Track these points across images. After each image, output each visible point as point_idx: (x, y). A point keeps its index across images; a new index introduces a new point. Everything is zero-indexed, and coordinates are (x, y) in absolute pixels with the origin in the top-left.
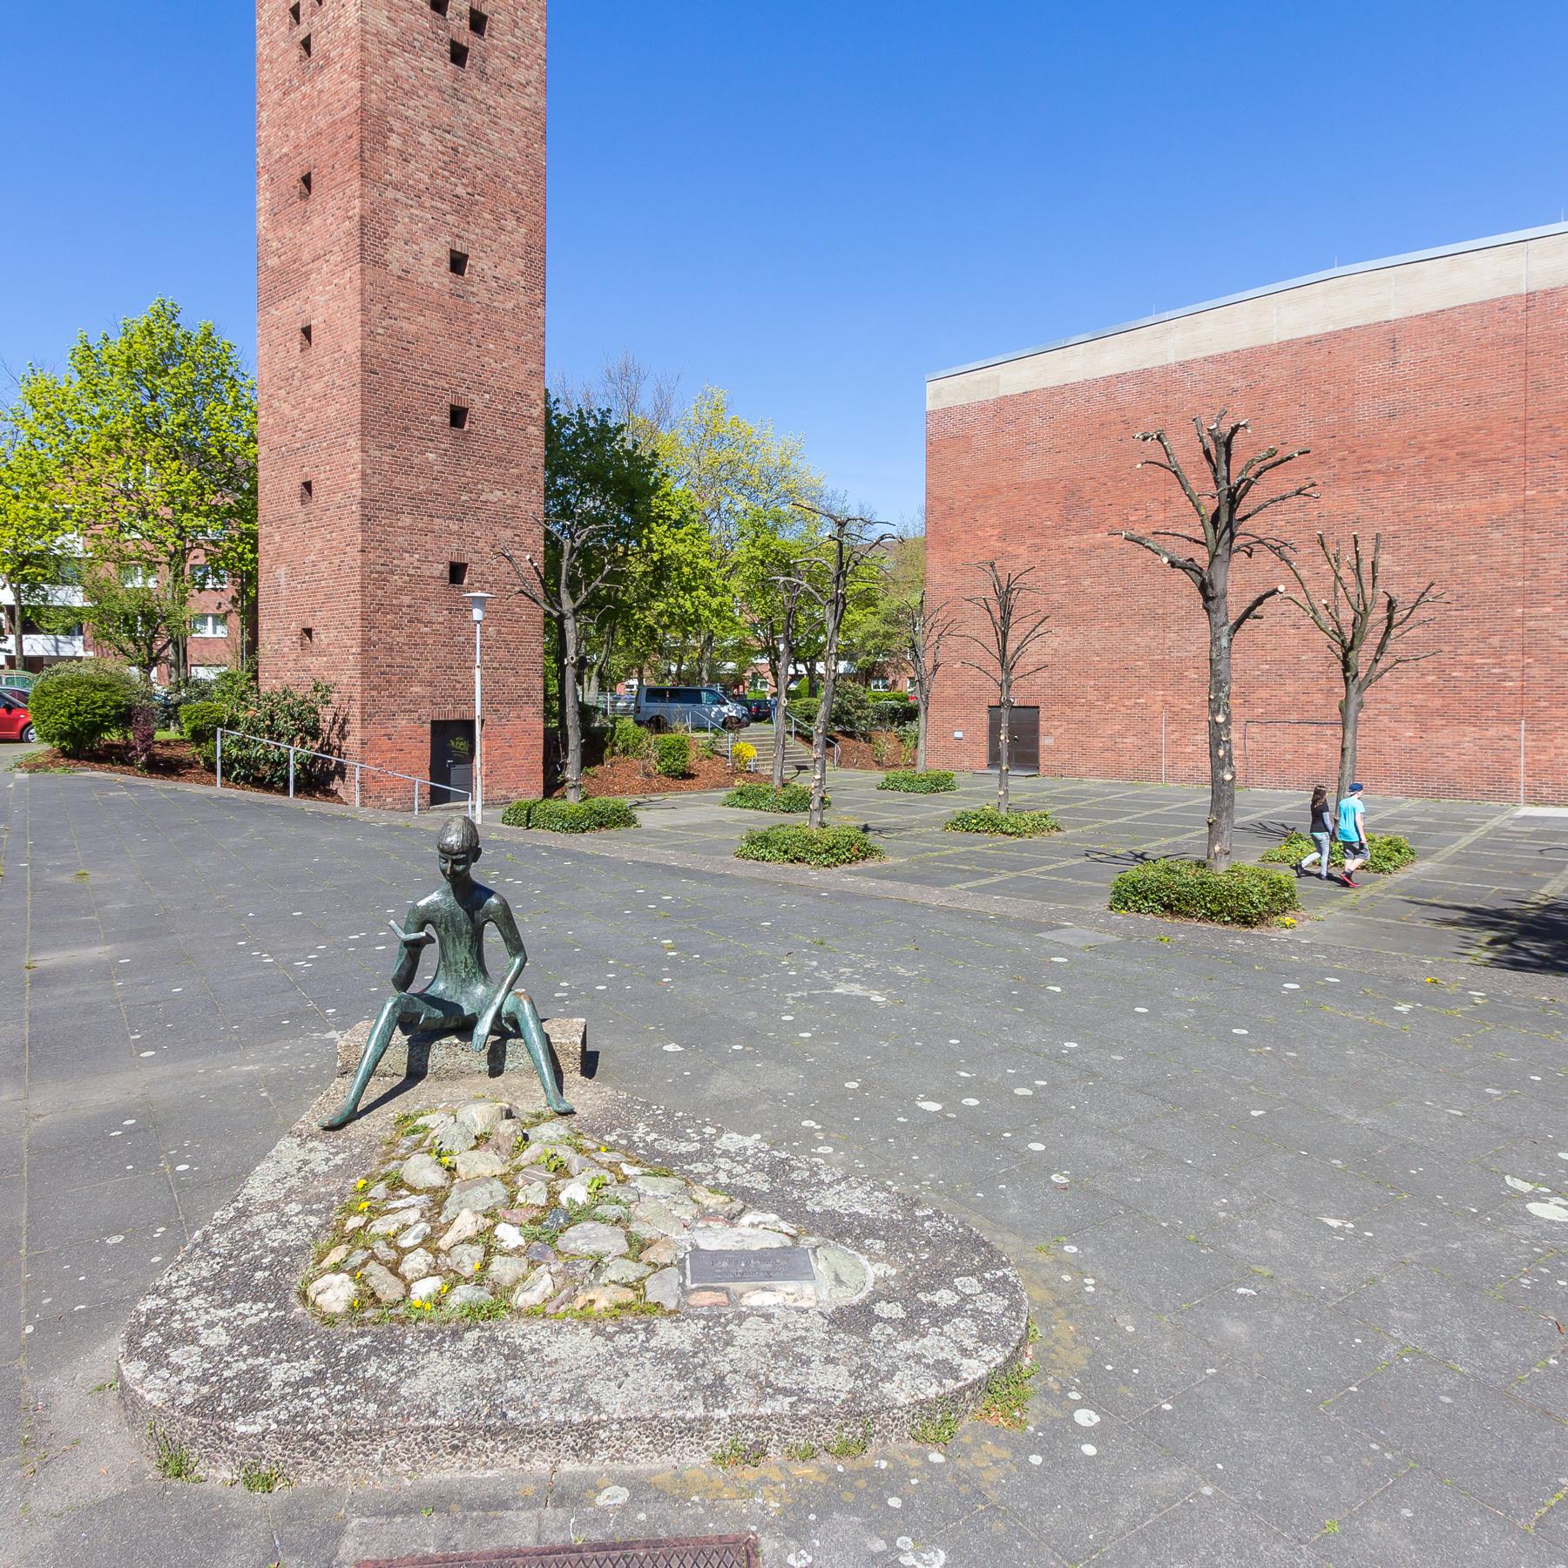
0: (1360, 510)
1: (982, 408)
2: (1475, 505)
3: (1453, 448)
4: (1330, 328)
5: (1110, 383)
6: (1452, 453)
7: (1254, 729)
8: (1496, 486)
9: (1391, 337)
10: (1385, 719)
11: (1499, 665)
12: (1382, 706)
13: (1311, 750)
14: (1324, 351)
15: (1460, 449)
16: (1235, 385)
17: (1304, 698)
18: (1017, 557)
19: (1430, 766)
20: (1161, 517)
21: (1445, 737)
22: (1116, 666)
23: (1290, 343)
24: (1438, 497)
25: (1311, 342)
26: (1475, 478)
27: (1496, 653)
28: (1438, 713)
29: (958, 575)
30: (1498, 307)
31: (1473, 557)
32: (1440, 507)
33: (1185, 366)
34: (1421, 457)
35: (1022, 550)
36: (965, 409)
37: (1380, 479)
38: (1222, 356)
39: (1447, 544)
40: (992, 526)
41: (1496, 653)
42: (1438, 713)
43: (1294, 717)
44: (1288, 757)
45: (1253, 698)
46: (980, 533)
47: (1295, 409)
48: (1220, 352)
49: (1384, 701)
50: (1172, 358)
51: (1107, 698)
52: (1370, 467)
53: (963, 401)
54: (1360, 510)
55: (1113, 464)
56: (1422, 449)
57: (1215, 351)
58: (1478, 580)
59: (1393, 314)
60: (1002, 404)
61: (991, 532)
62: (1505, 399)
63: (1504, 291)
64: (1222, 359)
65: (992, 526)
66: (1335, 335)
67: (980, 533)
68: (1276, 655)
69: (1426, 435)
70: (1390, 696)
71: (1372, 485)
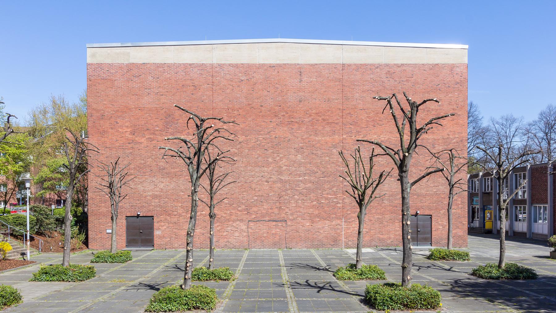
0: (290, 137)
1: (121, 67)
2: (328, 138)
3: (321, 117)
4: (278, 62)
5: (187, 67)
6: (320, 119)
7: (251, 224)
8: (334, 133)
9: (300, 70)
10: (300, 219)
11: (336, 198)
12: (298, 214)
13: (273, 232)
14: (276, 71)
15: (323, 117)
16: (242, 78)
17: (270, 211)
18: (141, 143)
19: (315, 236)
21: (319, 225)
23: (264, 65)
24: (316, 135)
25: (271, 66)
26: (328, 129)
27: (335, 194)
28: (318, 216)
29: (107, 149)
31: (327, 158)
32: (317, 139)
33: (221, 66)
34: (310, 119)
35: (143, 140)
36: (110, 65)
37: (297, 125)
38: (237, 65)
39: (319, 153)
40: (127, 127)
41: (335, 194)
42: (318, 216)
43: (267, 219)
44: (265, 235)
45: (251, 211)
46: (120, 130)
47: (265, 93)
48: (235, 63)
50: (215, 62)
52: (293, 120)
53: (109, 61)
54: (290, 137)
55: (189, 105)
56: (311, 116)
57: (234, 62)
58: (329, 166)
59: (301, 61)
60: (130, 67)
61: (126, 129)
62: (336, 101)
63: (335, 62)
64: (236, 66)
66: (279, 65)
67: (120, 130)
68: (260, 193)
69: (312, 110)
70: (301, 210)
71: (294, 127)
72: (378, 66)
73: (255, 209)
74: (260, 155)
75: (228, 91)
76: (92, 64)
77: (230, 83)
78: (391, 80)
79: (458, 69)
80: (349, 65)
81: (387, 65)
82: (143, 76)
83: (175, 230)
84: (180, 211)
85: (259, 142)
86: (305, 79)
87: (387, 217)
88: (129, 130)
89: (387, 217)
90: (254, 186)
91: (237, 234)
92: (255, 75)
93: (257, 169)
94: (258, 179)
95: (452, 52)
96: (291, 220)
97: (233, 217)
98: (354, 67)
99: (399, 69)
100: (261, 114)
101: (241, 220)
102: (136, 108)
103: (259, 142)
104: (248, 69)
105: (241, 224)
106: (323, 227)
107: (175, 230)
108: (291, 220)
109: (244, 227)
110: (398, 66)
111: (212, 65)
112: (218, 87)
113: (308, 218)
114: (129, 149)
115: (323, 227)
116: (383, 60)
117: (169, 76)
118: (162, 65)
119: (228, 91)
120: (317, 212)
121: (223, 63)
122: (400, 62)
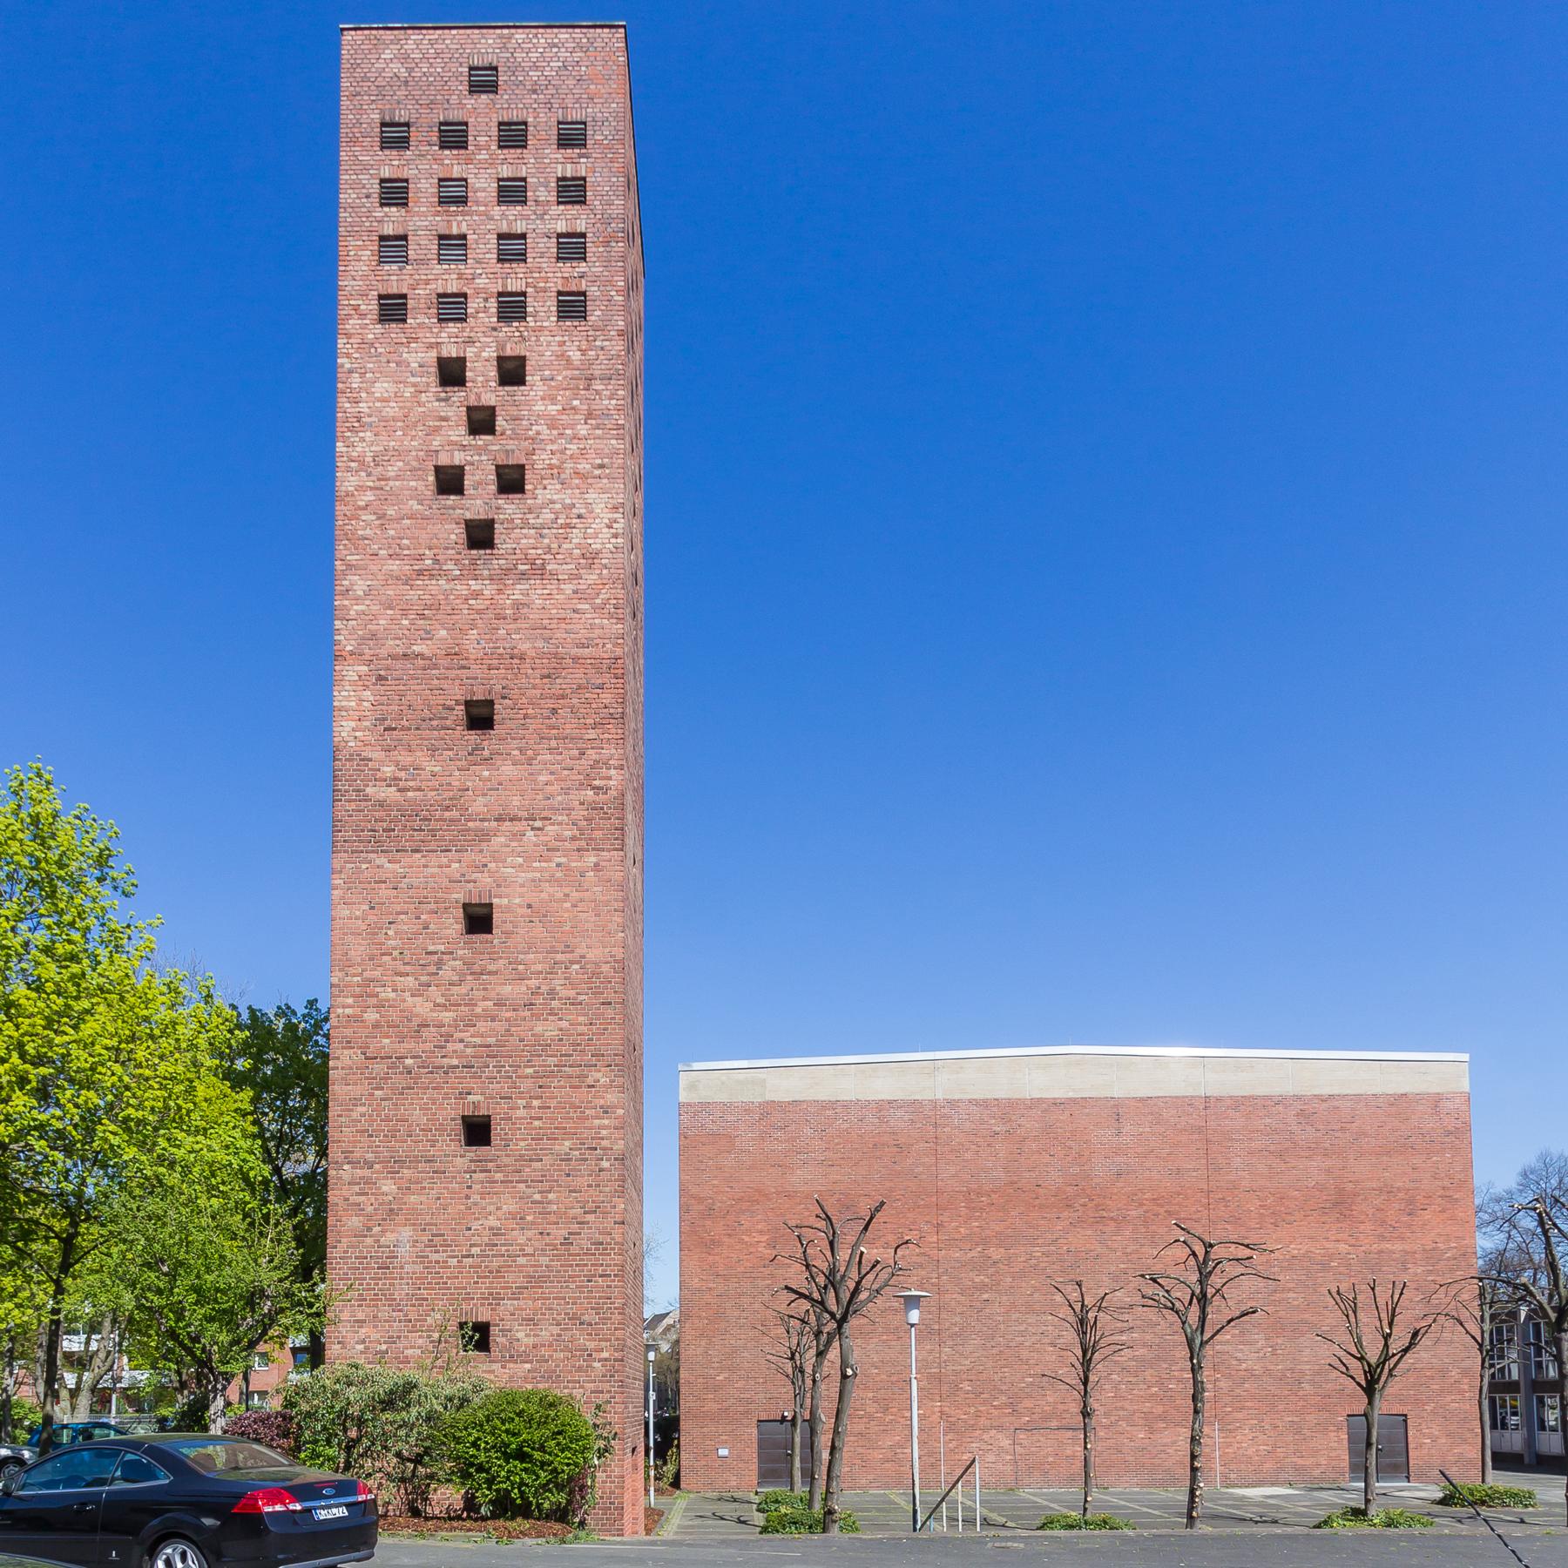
4: (1071, 1095)
6: (1162, 1210)
9: (1116, 1110)
13: (1069, 1452)
14: (1067, 1113)
15: (1167, 1207)
17: (1061, 1407)
20: (934, 1239)
22: (894, 1379)
25: (1057, 1104)
30: (1183, 1104)
33: (952, 1104)
34: (1141, 1211)
37: (1112, 1223)
38: (986, 1101)
43: (1054, 1424)
45: (1020, 1407)
47: (1046, 1158)
49: (1123, 1409)
50: (940, 1096)
51: (886, 1410)
55: (888, 1184)
56: (1141, 1205)
59: (1117, 1093)
64: (984, 1104)
65: (761, 1232)
66: (1074, 1101)
70: (1127, 1405)
71: (1106, 1229)
72: (1281, 1101)
73: (1028, 1403)
74: (1036, 1289)
75: (968, 1156)
76: (689, 1105)
77: (972, 1138)
78: (1308, 1128)
79: (1448, 1104)
80: (1219, 1099)
81: (1298, 1098)
82: (793, 1127)
83: (860, 1450)
84: (871, 1408)
85: (1034, 1261)
86: (1127, 1128)
87: (1312, 1418)
88: (764, 1238)
89: (1312, 1418)
90: (1025, 1354)
91: (991, 1458)
92: (1022, 1121)
93: (1032, 1319)
94: (1034, 1339)
95: (1435, 1070)
96: (1107, 1427)
97: (982, 1421)
98: (1229, 1102)
99: (1325, 1105)
100: (1037, 1202)
101: (1000, 1428)
102: (778, 1193)
103: (1034, 1261)
104: (1008, 1109)
105: (1000, 1436)
106: (1175, 1442)
107: (860, 1450)
108: (1107, 1427)
109: (1006, 1443)
110: (1323, 1099)
111: (934, 1103)
112: (946, 1148)
113: (1141, 1422)
114: (764, 1279)
115: (1175, 1442)
116: (1288, 1088)
117: (846, 1126)
118: (832, 1105)
119: (968, 1156)
120: (1160, 1409)
121: (956, 1097)
122: (1326, 1091)
